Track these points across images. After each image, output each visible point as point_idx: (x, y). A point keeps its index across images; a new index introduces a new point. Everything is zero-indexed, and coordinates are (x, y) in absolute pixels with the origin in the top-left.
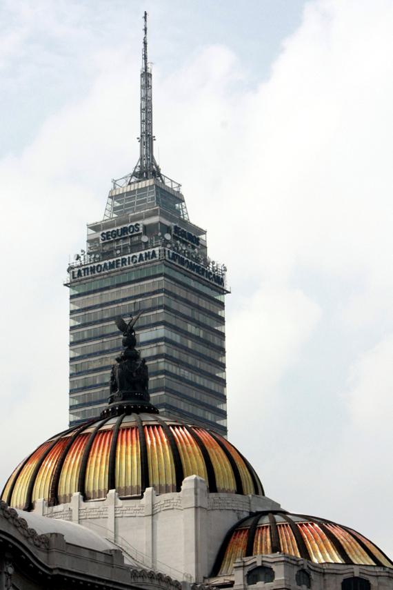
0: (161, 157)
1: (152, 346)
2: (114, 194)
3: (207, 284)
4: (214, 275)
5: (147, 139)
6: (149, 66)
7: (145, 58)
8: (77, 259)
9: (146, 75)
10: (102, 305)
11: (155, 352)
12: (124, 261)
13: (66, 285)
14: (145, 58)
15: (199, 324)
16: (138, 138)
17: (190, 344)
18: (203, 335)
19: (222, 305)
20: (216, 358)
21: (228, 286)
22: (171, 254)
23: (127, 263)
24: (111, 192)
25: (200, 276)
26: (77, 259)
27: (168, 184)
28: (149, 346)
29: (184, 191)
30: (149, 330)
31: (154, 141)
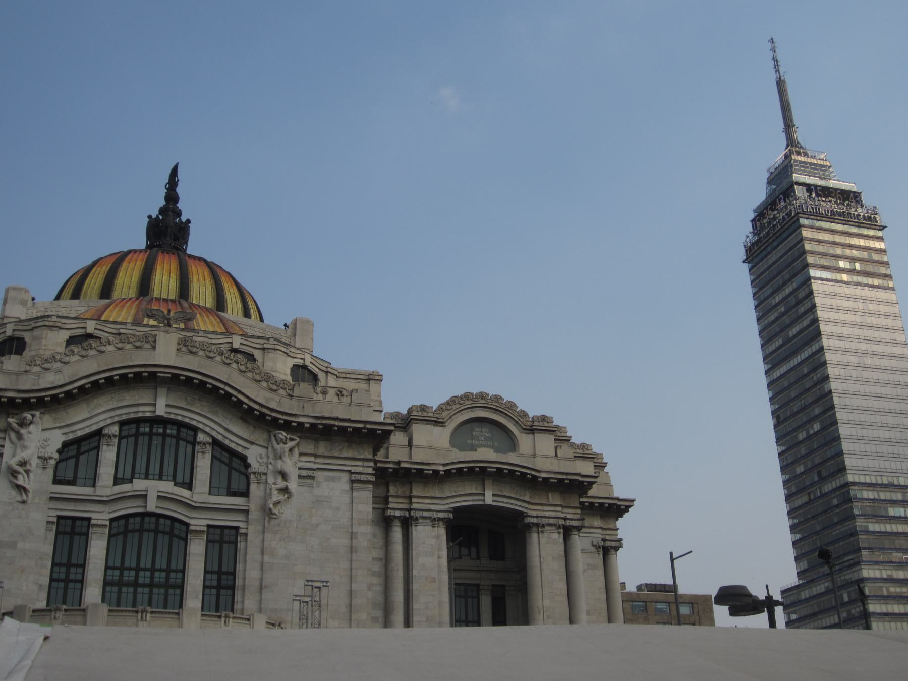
1: (804, 287)
2: (770, 180)
3: (857, 224)
5: (789, 125)
6: (782, 74)
7: (777, 70)
10: (768, 268)
11: (807, 291)
12: (774, 226)
13: (744, 262)
14: (777, 70)
16: (783, 131)
23: (776, 227)
25: (846, 219)
28: (802, 288)
30: (800, 274)
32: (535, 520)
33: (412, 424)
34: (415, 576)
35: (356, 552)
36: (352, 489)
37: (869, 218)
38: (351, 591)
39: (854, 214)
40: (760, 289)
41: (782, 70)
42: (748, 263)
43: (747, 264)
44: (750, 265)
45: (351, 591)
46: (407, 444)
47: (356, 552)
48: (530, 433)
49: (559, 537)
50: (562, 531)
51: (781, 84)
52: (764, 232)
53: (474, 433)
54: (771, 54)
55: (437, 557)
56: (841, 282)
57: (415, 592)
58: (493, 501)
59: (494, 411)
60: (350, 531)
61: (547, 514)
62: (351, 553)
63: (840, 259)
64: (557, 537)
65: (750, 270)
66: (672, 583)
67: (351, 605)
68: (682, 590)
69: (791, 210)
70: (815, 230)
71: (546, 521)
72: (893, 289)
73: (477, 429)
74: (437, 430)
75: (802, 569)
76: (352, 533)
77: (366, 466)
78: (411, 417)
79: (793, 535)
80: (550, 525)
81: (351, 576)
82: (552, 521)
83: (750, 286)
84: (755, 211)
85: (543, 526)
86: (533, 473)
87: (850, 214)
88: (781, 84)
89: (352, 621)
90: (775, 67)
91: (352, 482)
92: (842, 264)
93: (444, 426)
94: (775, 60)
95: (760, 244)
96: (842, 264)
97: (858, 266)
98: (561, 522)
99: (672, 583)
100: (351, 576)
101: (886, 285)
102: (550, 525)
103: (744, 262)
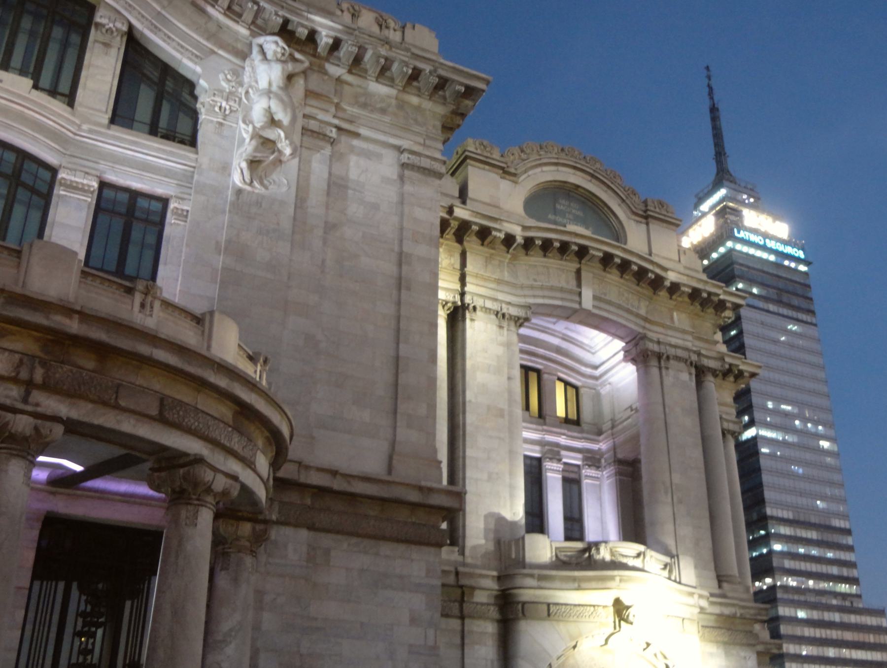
6: (716, 102)
7: (712, 98)
9: (714, 110)
14: (712, 98)
32: (656, 348)
33: (467, 166)
34: (470, 401)
35: (409, 289)
36: (401, 178)
38: (397, 358)
41: (716, 98)
45: (397, 358)
46: (457, 194)
47: (409, 289)
48: (641, 222)
49: (691, 379)
50: (693, 371)
53: (558, 206)
55: (506, 377)
56: (768, 311)
57: (469, 429)
58: (594, 306)
59: (589, 178)
60: (396, 248)
61: (673, 341)
62: (399, 289)
64: (687, 377)
67: (396, 384)
71: (672, 351)
72: (815, 325)
73: (563, 202)
74: (505, 185)
76: (401, 253)
77: (429, 147)
78: (467, 153)
80: (678, 359)
81: (398, 330)
82: (680, 353)
85: (668, 358)
86: (658, 271)
89: (399, 416)
91: (404, 166)
93: (516, 182)
94: (710, 87)
98: (694, 358)
100: (398, 330)
101: (809, 320)
102: (678, 359)
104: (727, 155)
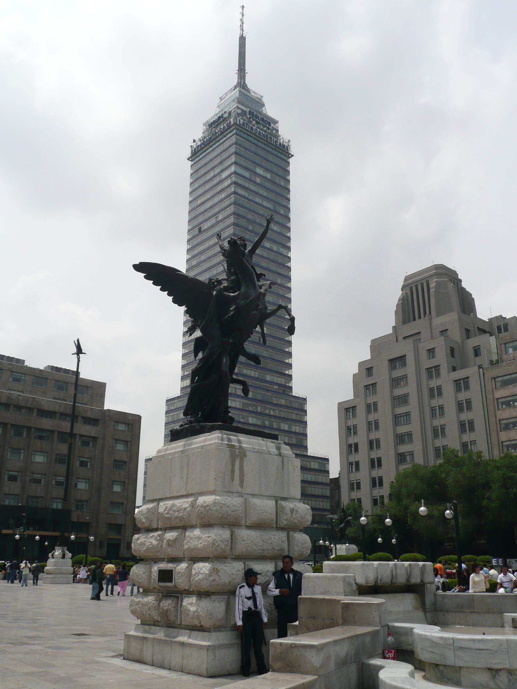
0: (249, 82)
4: (280, 143)
8: (194, 142)
13: (188, 159)
15: (266, 170)
17: (258, 180)
18: (270, 177)
19: (289, 163)
20: (285, 195)
21: (292, 151)
22: (241, 123)
24: (219, 104)
26: (194, 142)
27: (253, 94)
29: (264, 100)
31: (246, 74)
37: (284, 146)
39: (274, 139)
40: (197, 179)
42: (192, 161)
43: (190, 162)
44: (192, 163)
51: (242, 40)
52: (208, 138)
54: (240, 16)
63: (257, 166)
65: (192, 166)
66: (76, 370)
68: (82, 376)
69: (230, 121)
70: (245, 141)
75: (185, 385)
79: (183, 361)
83: (190, 177)
84: (204, 125)
87: (271, 138)
88: (242, 40)
90: (241, 26)
92: (259, 170)
95: (203, 146)
96: (259, 170)
97: (268, 176)
99: (76, 370)
103: (188, 159)
104: (246, 72)
